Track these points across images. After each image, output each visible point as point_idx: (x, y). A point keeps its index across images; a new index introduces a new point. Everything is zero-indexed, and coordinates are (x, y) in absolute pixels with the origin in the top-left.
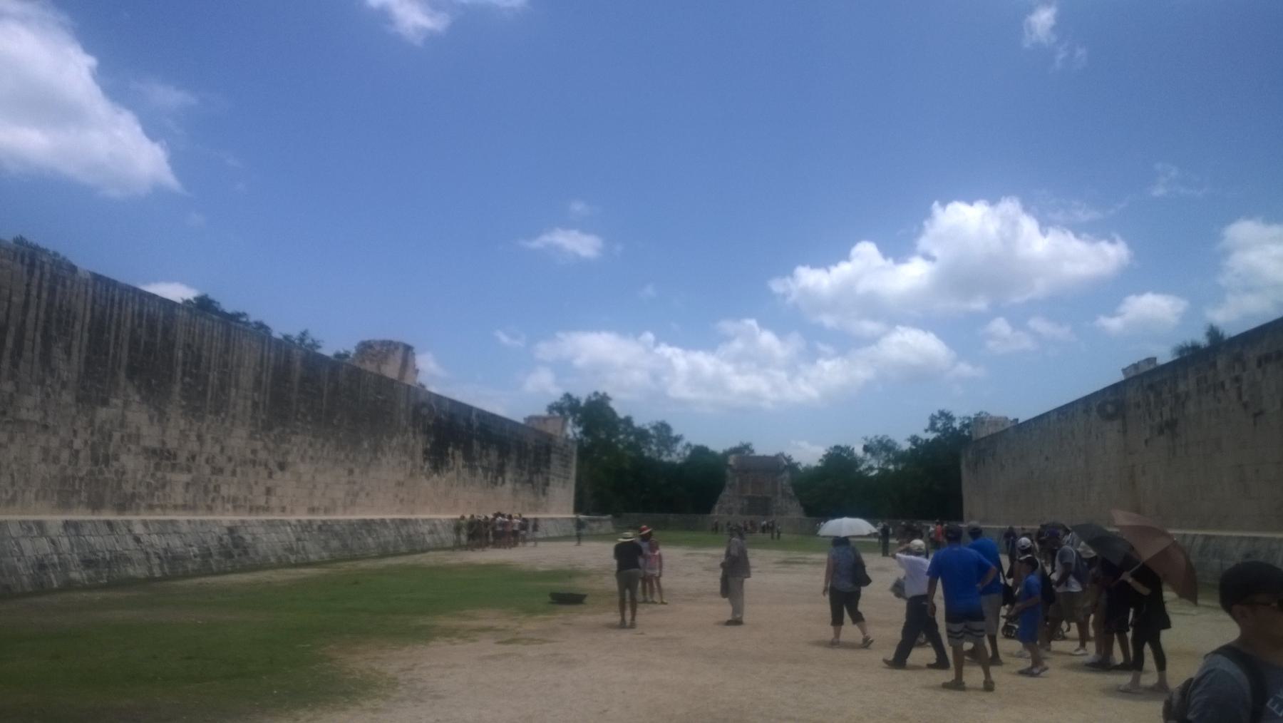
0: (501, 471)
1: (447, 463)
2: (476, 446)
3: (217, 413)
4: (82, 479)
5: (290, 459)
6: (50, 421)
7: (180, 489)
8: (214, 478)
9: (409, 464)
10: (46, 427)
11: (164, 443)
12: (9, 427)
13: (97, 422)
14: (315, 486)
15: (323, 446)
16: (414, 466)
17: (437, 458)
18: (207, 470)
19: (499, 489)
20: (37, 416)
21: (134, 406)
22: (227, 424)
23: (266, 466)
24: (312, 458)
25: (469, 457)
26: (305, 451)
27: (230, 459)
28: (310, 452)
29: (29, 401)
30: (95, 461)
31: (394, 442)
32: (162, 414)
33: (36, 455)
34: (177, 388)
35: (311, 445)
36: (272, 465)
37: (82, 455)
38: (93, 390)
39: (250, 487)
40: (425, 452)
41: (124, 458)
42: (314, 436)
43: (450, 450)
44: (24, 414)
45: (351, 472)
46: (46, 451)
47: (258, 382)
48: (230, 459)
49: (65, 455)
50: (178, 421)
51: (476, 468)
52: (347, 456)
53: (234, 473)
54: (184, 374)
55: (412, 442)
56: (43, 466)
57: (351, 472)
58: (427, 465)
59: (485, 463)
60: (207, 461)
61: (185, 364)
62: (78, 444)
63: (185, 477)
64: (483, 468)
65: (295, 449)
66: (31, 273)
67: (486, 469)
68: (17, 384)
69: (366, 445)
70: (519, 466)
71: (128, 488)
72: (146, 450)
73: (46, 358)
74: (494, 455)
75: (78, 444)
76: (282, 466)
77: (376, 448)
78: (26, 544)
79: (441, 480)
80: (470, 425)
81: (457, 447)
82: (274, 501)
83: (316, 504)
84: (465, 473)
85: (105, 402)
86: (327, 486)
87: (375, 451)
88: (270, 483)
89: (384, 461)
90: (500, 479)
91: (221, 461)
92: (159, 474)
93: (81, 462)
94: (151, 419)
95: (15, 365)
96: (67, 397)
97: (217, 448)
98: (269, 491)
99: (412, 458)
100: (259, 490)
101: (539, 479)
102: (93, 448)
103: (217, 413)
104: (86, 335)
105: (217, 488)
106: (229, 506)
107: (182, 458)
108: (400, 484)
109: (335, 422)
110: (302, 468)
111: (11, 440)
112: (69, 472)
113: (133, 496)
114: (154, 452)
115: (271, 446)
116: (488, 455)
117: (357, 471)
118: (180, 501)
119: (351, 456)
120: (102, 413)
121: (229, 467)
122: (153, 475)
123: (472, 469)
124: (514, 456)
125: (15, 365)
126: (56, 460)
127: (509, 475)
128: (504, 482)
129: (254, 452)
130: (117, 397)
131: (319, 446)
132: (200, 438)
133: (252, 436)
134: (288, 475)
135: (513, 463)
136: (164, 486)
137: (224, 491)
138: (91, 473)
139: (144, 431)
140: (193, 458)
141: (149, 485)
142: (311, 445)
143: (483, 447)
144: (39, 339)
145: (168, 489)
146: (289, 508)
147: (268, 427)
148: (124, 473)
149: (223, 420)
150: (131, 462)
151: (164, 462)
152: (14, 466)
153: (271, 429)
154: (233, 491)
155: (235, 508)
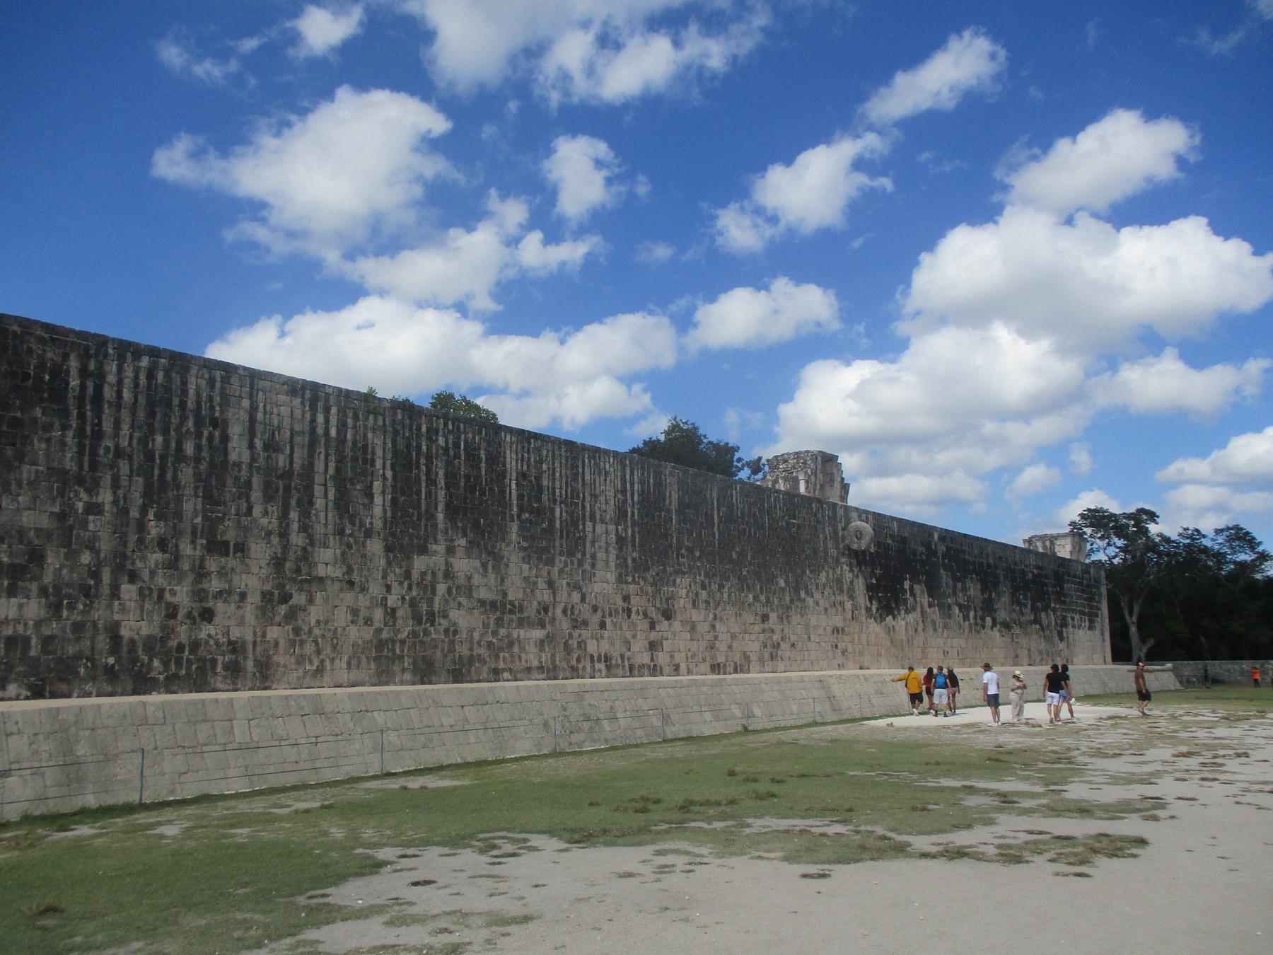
1: (905, 600)
2: (945, 577)
3: (571, 553)
4: (403, 642)
6: (355, 577)
7: (532, 649)
8: (576, 633)
9: (848, 605)
10: (351, 584)
11: (505, 594)
13: (415, 575)
14: (716, 637)
15: (721, 587)
16: (855, 607)
17: (887, 598)
18: (566, 625)
21: (460, 552)
22: (587, 567)
23: (645, 615)
24: (707, 602)
25: (933, 590)
26: (697, 595)
27: (595, 609)
28: (704, 595)
29: (327, 555)
30: (418, 619)
31: (823, 577)
32: (498, 558)
33: (342, 618)
34: (514, 527)
35: (704, 587)
36: (652, 612)
37: (399, 613)
38: (405, 537)
39: (627, 643)
40: (869, 588)
41: (454, 614)
43: (907, 585)
44: (321, 571)
46: (355, 612)
47: (621, 514)
48: (595, 609)
49: (378, 615)
50: (517, 569)
51: (950, 607)
52: (756, 598)
53: (603, 625)
54: (521, 509)
56: (353, 630)
57: (765, 618)
60: (564, 612)
61: (520, 497)
62: (392, 600)
63: (538, 634)
64: (961, 607)
66: (313, 408)
69: (782, 583)
71: (463, 650)
72: (482, 603)
74: (974, 590)
75: (392, 600)
76: (668, 615)
77: (797, 586)
80: (932, 552)
82: (662, 658)
83: (721, 659)
84: (934, 614)
85: (423, 550)
86: (734, 637)
87: (797, 591)
88: (653, 636)
89: (810, 601)
90: (988, 619)
91: (585, 611)
92: (502, 631)
93: (399, 622)
94: (484, 566)
96: (375, 547)
97: (576, 597)
98: (653, 646)
99: (851, 597)
100: (639, 645)
101: (1049, 618)
102: (413, 603)
103: (571, 553)
104: (389, 474)
105: (582, 645)
106: (602, 666)
107: (531, 611)
108: (836, 630)
109: (734, 555)
110: (695, 615)
111: (311, 601)
112: (384, 635)
113: (471, 660)
114: (493, 604)
115: (650, 589)
116: (964, 589)
118: (535, 664)
119: (763, 598)
120: (419, 564)
121: (595, 620)
122: (495, 633)
123: (946, 611)
124: (1005, 588)
126: (368, 621)
129: (626, 598)
130: (436, 542)
131: (715, 587)
132: (551, 584)
133: (620, 580)
134: (677, 625)
135: (1005, 599)
136: (511, 644)
137: (592, 647)
138: (414, 634)
139: (477, 580)
140: (546, 610)
141: (490, 644)
145: (516, 649)
146: (683, 666)
147: (641, 567)
148: (455, 632)
149: (581, 563)
150: (464, 619)
151: (507, 617)
152: (317, 631)
153: (647, 569)
154: (605, 647)
155: (608, 667)
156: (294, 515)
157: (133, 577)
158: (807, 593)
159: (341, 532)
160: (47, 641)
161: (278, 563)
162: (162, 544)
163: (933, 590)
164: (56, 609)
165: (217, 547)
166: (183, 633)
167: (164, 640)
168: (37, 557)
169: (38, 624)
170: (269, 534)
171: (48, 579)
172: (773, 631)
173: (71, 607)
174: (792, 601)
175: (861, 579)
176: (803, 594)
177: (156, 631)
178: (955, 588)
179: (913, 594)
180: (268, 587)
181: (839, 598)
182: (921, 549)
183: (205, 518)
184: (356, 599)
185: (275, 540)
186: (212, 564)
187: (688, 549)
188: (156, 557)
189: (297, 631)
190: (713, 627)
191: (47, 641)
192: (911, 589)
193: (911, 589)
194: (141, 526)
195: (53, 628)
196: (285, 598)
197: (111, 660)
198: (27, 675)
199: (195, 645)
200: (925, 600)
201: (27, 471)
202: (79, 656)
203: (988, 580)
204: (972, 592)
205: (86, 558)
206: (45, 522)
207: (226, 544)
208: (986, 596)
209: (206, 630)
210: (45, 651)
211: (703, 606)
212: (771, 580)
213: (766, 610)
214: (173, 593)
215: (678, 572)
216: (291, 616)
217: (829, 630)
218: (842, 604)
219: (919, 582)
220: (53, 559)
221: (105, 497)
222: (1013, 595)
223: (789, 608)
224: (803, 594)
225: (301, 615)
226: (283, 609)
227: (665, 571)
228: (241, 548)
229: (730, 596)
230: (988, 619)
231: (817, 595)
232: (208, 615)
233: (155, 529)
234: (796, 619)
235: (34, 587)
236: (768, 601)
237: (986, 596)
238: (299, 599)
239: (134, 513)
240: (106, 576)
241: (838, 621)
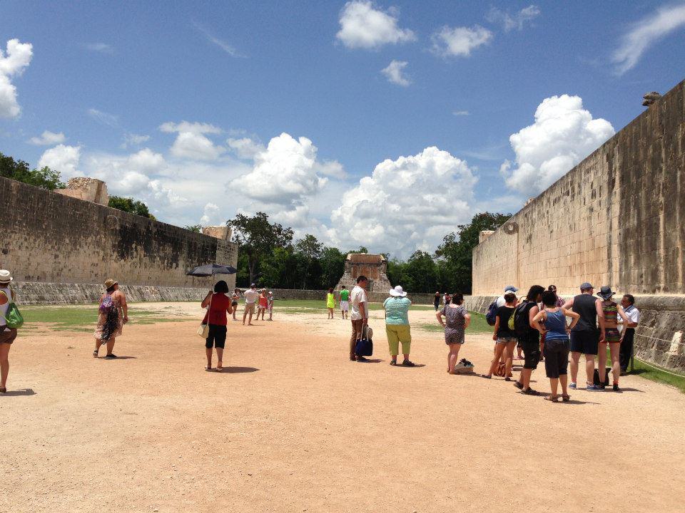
0: (175, 259)
1: (132, 254)
5: (11, 248)
9: (102, 253)
15: (35, 240)
16: (106, 255)
17: (123, 250)
19: (173, 270)
24: (27, 247)
25: (146, 250)
31: (89, 240)
35: (26, 240)
40: (114, 246)
42: (28, 234)
43: (134, 246)
45: (56, 256)
52: (53, 247)
55: (104, 240)
57: (56, 256)
58: (115, 254)
59: (162, 254)
65: (14, 242)
67: (162, 259)
69: (67, 241)
70: (190, 256)
74: (169, 250)
79: (127, 264)
80: (149, 231)
81: (139, 243)
83: (31, 274)
84: (146, 260)
87: (75, 245)
90: (174, 265)
99: (103, 250)
109: (44, 227)
110: (20, 253)
117: (61, 256)
123: (152, 258)
124: (185, 250)
127: (181, 263)
128: (177, 266)
131: (31, 240)
142: (26, 240)
143: (160, 245)
158: (80, 246)
163: (147, 249)
172: (60, 263)
174: (72, 250)
175: (110, 241)
176: (78, 247)
178: (159, 249)
179: (136, 251)
181: (96, 250)
182: (143, 229)
187: (20, 222)
190: (29, 259)
192: (136, 248)
193: (136, 248)
200: (142, 253)
203: (177, 246)
204: (167, 251)
208: (175, 253)
211: (24, 249)
212: (61, 240)
213: (58, 253)
215: (12, 232)
217: (90, 265)
218: (98, 253)
219: (141, 245)
222: (189, 254)
223: (70, 253)
224: (78, 247)
227: (6, 231)
229: (39, 245)
230: (174, 265)
231: (86, 248)
234: (72, 258)
236: (59, 248)
237: (175, 253)
241: (95, 261)
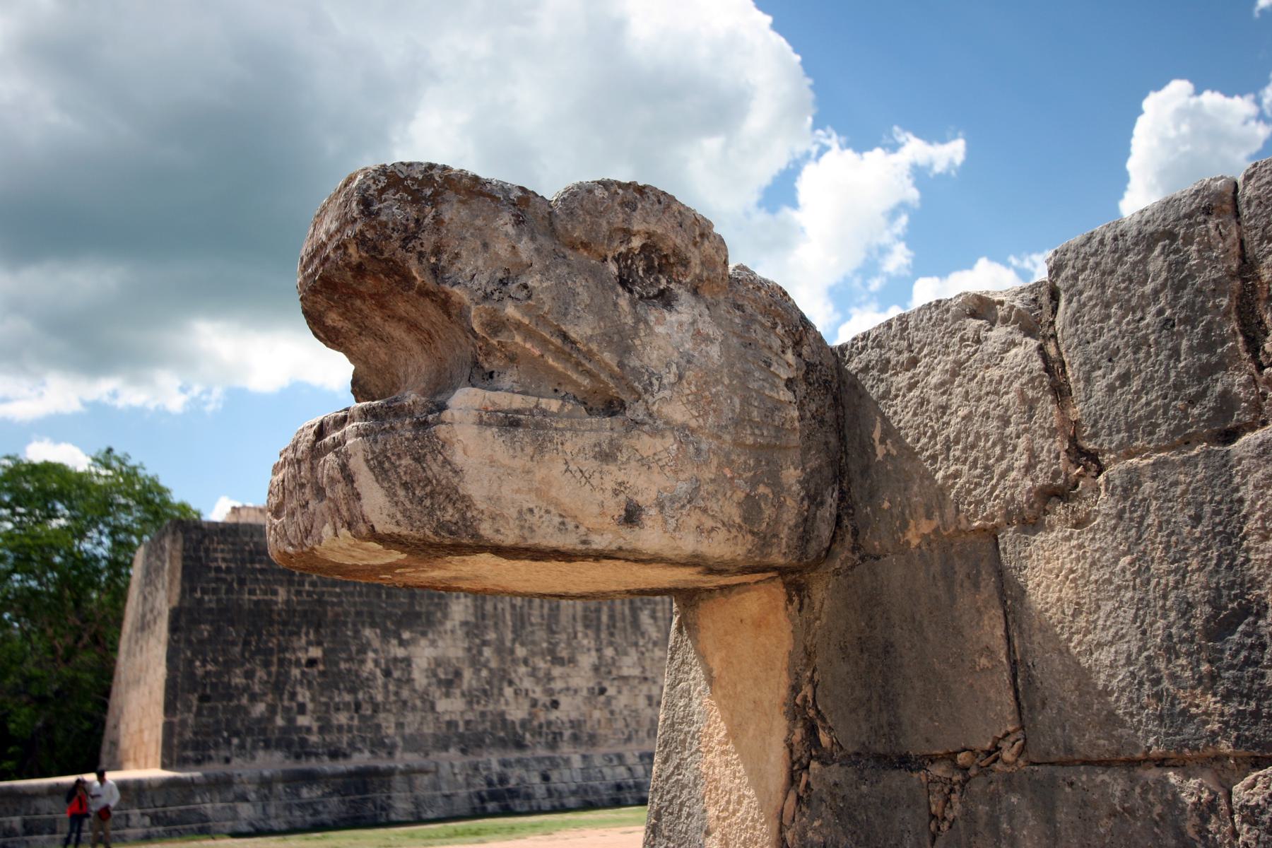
6: (648, 675)
10: (646, 679)
12: (616, 683)
20: (636, 672)
44: (626, 672)
46: (650, 698)
68: (616, 650)
73: (636, 623)
78: (607, 771)
95: (612, 635)
111: (619, 692)
125: (612, 635)
144: (627, 611)
156: (603, 635)
157: (511, 683)
159: (636, 644)
160: (468, 723)
161: (596, 669)
162: (526, 662)
164: (470, 703)
165: (558, 661)
166: (542, 716)
167: (530, 721)
168: (458, 674)
169: (462, 713)
170: (589, 650)
171: (465, 686)
173: (478, 703)
177: (527, 717)
180: (591, 685)
183: (550, 643)
184: (650, 690)
185: (593, 653)
186: (557, 671)
188: (522, 670)
189: (612, 712)
191: (468, 723)
194: (512, 651)
195: (470, 716)
196: (603, 691)
197: (502, 734)
198: (460, 742)
199: (549, 723)
201: (449, 625)
202: (485, 731)
205: (484, 673)
206: (460, 653)
207: (562, 659)
209: (554, 715)
210: (467, 729)
214: (534, 692)
216: (609, 701)
220: (467, 674)
221: (491, 636)
225: (614, 702)
226: (602, 698)
228: (572, 660)
232: (555, 704)
233: (521, 652)
235: (458, 692)
238: (611, 691)
239: (508, 644)
240: (496, 682)
